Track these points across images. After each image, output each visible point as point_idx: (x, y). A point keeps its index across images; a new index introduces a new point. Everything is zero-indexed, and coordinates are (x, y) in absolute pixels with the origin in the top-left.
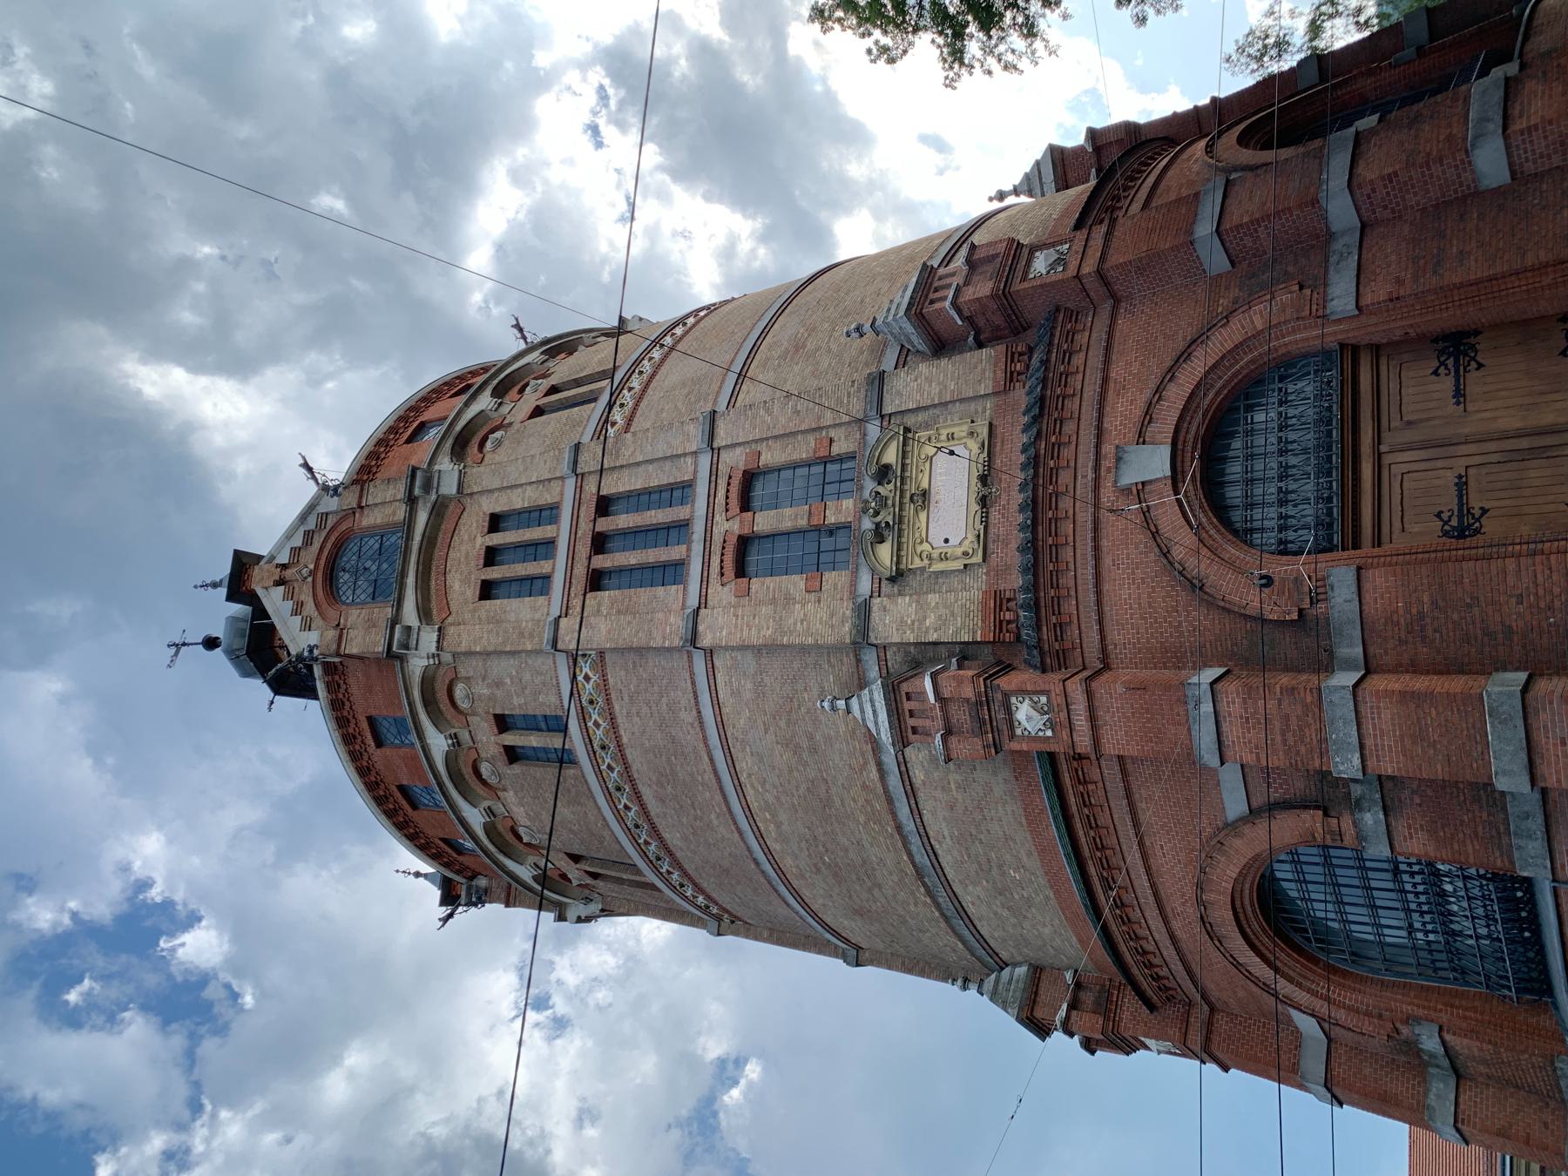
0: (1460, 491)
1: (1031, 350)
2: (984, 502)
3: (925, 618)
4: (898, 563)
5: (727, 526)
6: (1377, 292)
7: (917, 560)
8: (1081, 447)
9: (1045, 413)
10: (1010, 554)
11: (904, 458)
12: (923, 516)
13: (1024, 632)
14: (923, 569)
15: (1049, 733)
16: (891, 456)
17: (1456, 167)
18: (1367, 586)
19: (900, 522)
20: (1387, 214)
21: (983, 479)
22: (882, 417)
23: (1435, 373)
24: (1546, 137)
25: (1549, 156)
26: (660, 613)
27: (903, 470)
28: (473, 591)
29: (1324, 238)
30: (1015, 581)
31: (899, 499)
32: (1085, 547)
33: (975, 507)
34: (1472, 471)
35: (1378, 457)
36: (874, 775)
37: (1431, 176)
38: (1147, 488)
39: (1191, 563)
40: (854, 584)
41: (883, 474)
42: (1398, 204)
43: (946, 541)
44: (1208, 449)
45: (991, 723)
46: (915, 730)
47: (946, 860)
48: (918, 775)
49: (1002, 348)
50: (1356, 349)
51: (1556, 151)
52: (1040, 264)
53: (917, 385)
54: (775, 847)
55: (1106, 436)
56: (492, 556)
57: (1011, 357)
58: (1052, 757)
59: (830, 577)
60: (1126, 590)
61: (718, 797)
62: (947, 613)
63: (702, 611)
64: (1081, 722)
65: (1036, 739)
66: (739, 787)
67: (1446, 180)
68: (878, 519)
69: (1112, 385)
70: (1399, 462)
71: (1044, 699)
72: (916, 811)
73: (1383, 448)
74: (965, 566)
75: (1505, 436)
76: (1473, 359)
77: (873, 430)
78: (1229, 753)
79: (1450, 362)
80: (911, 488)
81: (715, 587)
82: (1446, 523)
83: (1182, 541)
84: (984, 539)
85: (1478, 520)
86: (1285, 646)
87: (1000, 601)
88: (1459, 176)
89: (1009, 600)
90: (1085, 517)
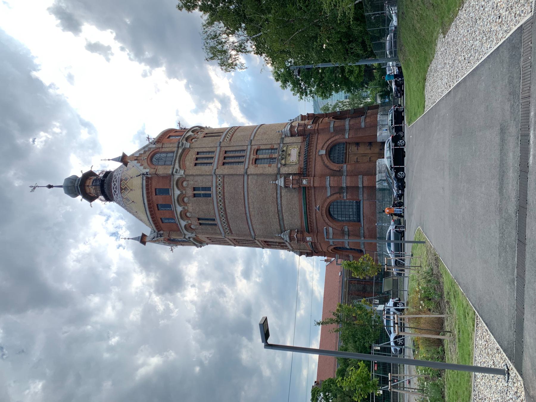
2: (299, 156)
6: (351, 136)
9: (309, 145)
10: (302, 163)
16: (285, 149)
26: (240, 169)
28: (192, 164)
29: (344, 130)
31: (285, 154)
36: (275, 194)
40: (277, 166)
41: (283, 151)
44: (330, 152)
45: (299, 182)
47: (283, 208)
48: (283, 194)
52: (309, 127)
53: (288, 140)
54: (251, 210)
56: (197, 159)
57: (304, 138)
59: (273, 165)
60: (318, 167)
61: (243, 201)
62: (294, 169)
64: (312, 182)
66: (248, 199)
72: (281, 200)
77: (282, 145)
81: (251, 166)
84: (299, 160)
86: (338, 173)
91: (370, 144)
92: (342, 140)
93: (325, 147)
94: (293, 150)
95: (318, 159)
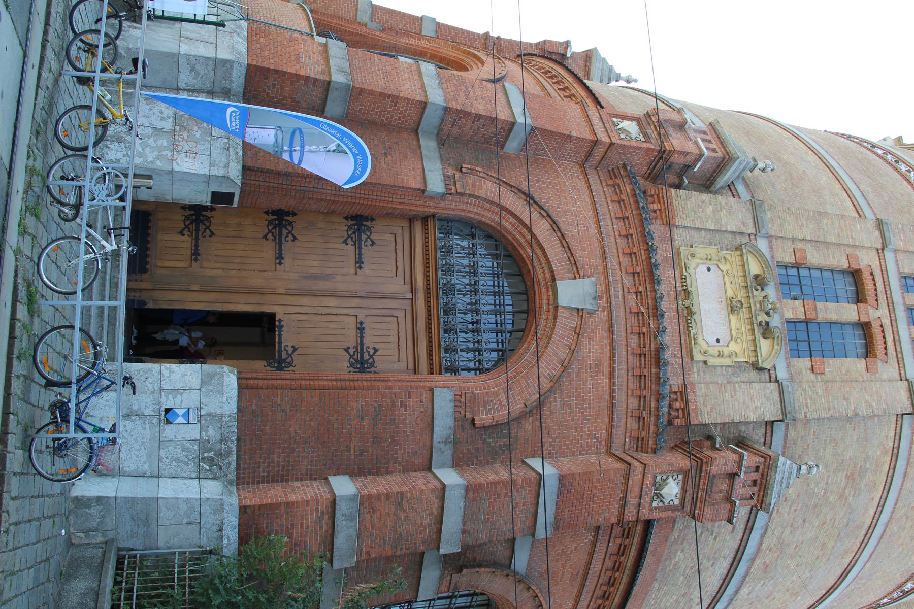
0: (360, 258)
4: (742, 255)
5: (878, 313)
7: (728, 257)
11: (754, 340)
16: (765, 345)
22: (777, 381)
23: (376, 350)
27: (753, 329)
34: (353, 271)
38: (572, 275)
39: (535, 215)
41: (767, 331)
43: (709, 269)
52: (672, 490)
55: (606, 327)
59: (789, 259)
63: (880, 246)
68: (763, 294)
69: (606, 372)
70: (398, 286)
74: (692, 246)
76: (351, 356)
79: (366, 357)
81: (875, 265)
82: (369, 237)
83: (542, 229)
85: (349, 236)
93: (566, 322)
95: (587, 256)
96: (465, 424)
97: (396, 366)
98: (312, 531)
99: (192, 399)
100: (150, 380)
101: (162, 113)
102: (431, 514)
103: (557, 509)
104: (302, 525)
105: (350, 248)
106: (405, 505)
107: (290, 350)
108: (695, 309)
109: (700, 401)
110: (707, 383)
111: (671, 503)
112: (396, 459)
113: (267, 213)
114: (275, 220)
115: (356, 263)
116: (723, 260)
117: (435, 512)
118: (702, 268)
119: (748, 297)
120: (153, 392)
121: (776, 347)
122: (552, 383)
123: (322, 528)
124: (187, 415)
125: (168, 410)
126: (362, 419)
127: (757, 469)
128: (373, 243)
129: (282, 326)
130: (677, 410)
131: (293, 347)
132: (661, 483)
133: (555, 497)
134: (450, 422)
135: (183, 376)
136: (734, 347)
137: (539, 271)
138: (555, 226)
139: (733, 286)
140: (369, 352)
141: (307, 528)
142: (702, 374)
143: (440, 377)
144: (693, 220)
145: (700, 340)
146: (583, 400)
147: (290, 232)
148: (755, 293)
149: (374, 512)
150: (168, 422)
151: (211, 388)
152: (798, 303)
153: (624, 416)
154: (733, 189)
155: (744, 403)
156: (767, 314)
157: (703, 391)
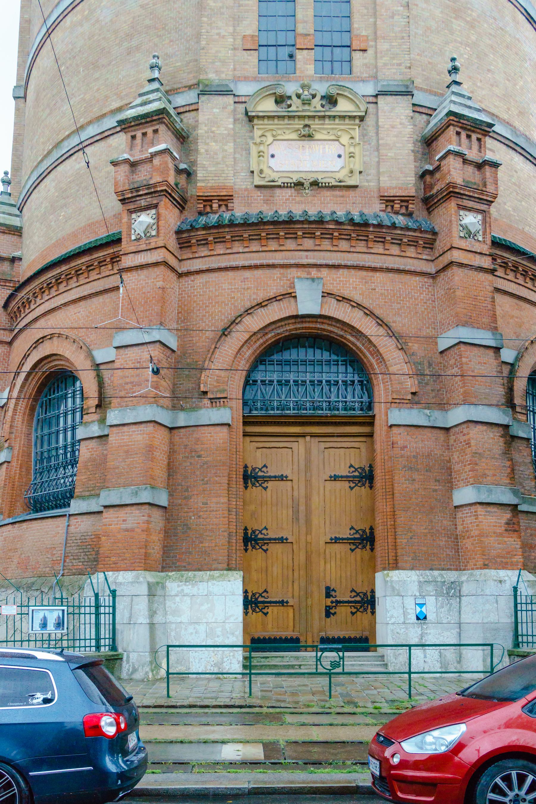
0: (278, 477)
1: (410, 215)
2: (299, 184)
3: (216, 141)
4: (258, 117)
6: (400, 437)
7: (260, 133)
8: (329, 254)
9: (359, 229)
11: (340, 117)
12: (294, 136)
13: (204, 218)
14: (252, 138)
15: (133, 237)
17: (466, 479)
18: (218, 428)
19: (290, 117)
20: (451, 442)
21: (315, 184)
22: (376, 96)
24: (471, 523)
25: (462, 525)
27: (330, 117)
29: (443, 406)
30: (239, 210)
31: (306, 115)
32: (256, 259)
33: (295, 178)
34: (289, 483)
35: (303, 436)
37: (465, 466)
38: (292, 300)
39: (239, 327)
40: (246, 79)
42: (456, 448)
43: (273, 156)
46: (134, 137)
49: (412, 193)
50: (371, 424)
51: (464, 528)
52: (471, 220)
53: (398, 126)
55: (334, 271)
57: (405, 200)
58: (119, 241)
64: (141, 259)
65: (130, 228)
67: (462, 473)
68: (294, 98)
71: (154, 233)
73: (308, 438)
74: (252, 172)
75: (308, 498)
77: (369, 89)
78: (122, 351)
80: (315, 124)
82: (260, 470)
85: (260, 485)
87: (225, 200)
88: (463, 480)
89: (226, 206)
90: (278, 259)
91: (366, 540)
92: (381, 393)
93: (335, 310)
94: (333, 149)
95: (272, 283)
96: (414, 399)
97: (363, 450)
98: (498, 519)
99: (410, 603)
100: (398, 631)
101: (192, 633)
102: (486, 431)
103: (483, 328)
104: (494, 526)
105: (270, 484)
106: (480, 451)
107: (353, 531)
108: (312, 177)
109: (394, 183)
110: (379, 174)
111: (480, 223)
112: (441, 455)
113: (246, 550)
114: (251, 544)
115: (282, 480)
116: (263, 139)
117: (485, 428)
118: (272, 162)
119: (299, 117)
120: (407, 628)
121: (346, 94)
122: (383, 325)
123: (495, 512)
124: (421, 605)
125: (418, 618)
126: (414, 480)
127: (458, 133)
128: (265, 466)
129: (336, 537)
130: (401, 206)
131: (350, 529)
132: (465, 231)
133: (475, 330)
134: (415, 412)
135: (394, 608)
136: (345, 139)
137: (288, 328)
138: (248, 312)
139: (287, 132)
140: (353, 472)
141: (496, 522)
142: (369, 178)
143: (377, 417)
144: (227, 166)
145: (340, 176)
146: (394, 296)
147: (260, 532)
148: (293, 108)
149: (485, 474)
150: (425, 618)
151: (401, 589)
152: (300, 56)
153: (406, 260)
154: (182, 110)
155: (396, 136)
156: (314, 96)
157: (387, 179)
